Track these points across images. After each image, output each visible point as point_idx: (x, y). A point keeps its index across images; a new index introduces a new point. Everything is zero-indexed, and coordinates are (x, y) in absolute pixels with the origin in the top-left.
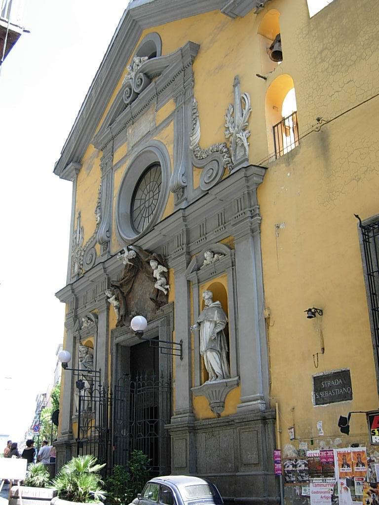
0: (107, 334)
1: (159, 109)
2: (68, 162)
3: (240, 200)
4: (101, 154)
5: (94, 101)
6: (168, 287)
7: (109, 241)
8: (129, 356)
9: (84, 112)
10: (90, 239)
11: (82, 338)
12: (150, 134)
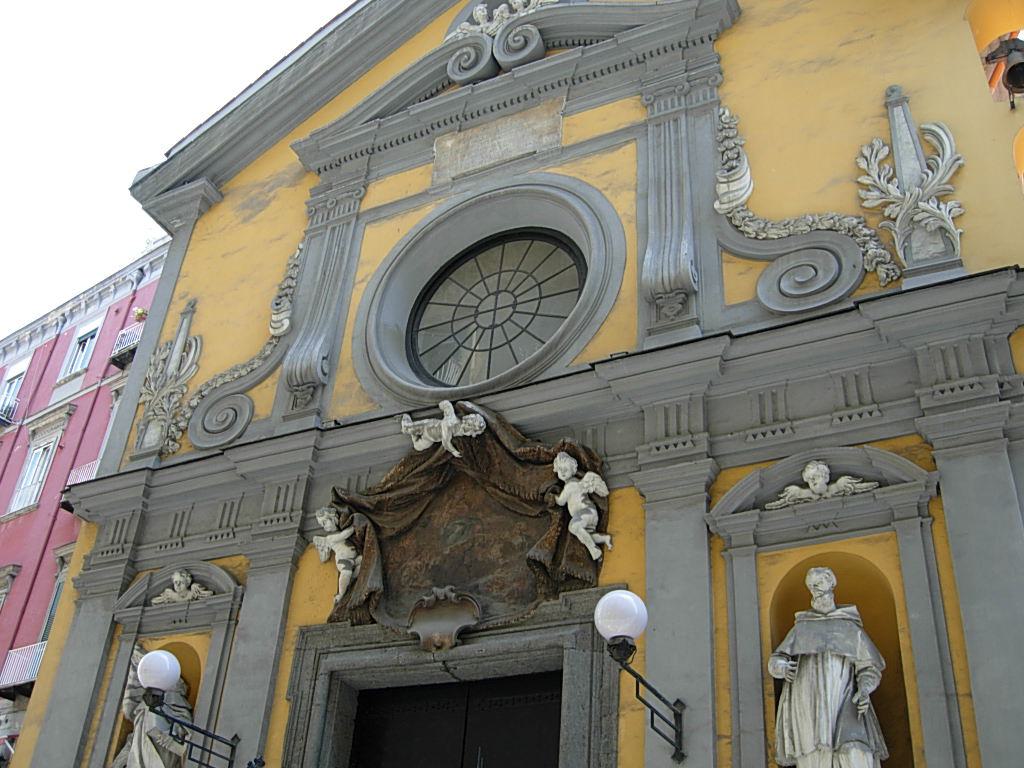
0: (282, 637)
1: (571, 113)
2: (180, 180)
3: (678, 413)
4: (312, 181)
5: (327, 59)
6: (606, 539)
7: (324, 385)
8: (354, 717)
9: (284, 78)
10: (236, 370)
11: (144, 629)
12: (535, 159)
